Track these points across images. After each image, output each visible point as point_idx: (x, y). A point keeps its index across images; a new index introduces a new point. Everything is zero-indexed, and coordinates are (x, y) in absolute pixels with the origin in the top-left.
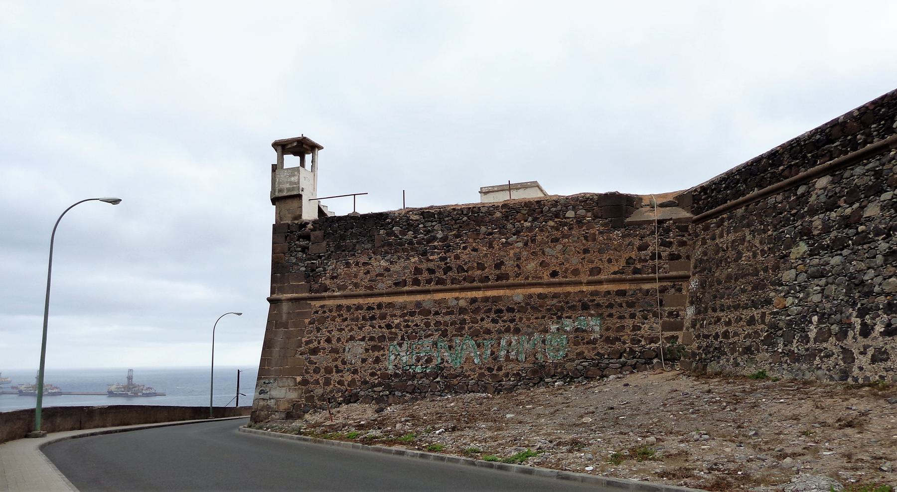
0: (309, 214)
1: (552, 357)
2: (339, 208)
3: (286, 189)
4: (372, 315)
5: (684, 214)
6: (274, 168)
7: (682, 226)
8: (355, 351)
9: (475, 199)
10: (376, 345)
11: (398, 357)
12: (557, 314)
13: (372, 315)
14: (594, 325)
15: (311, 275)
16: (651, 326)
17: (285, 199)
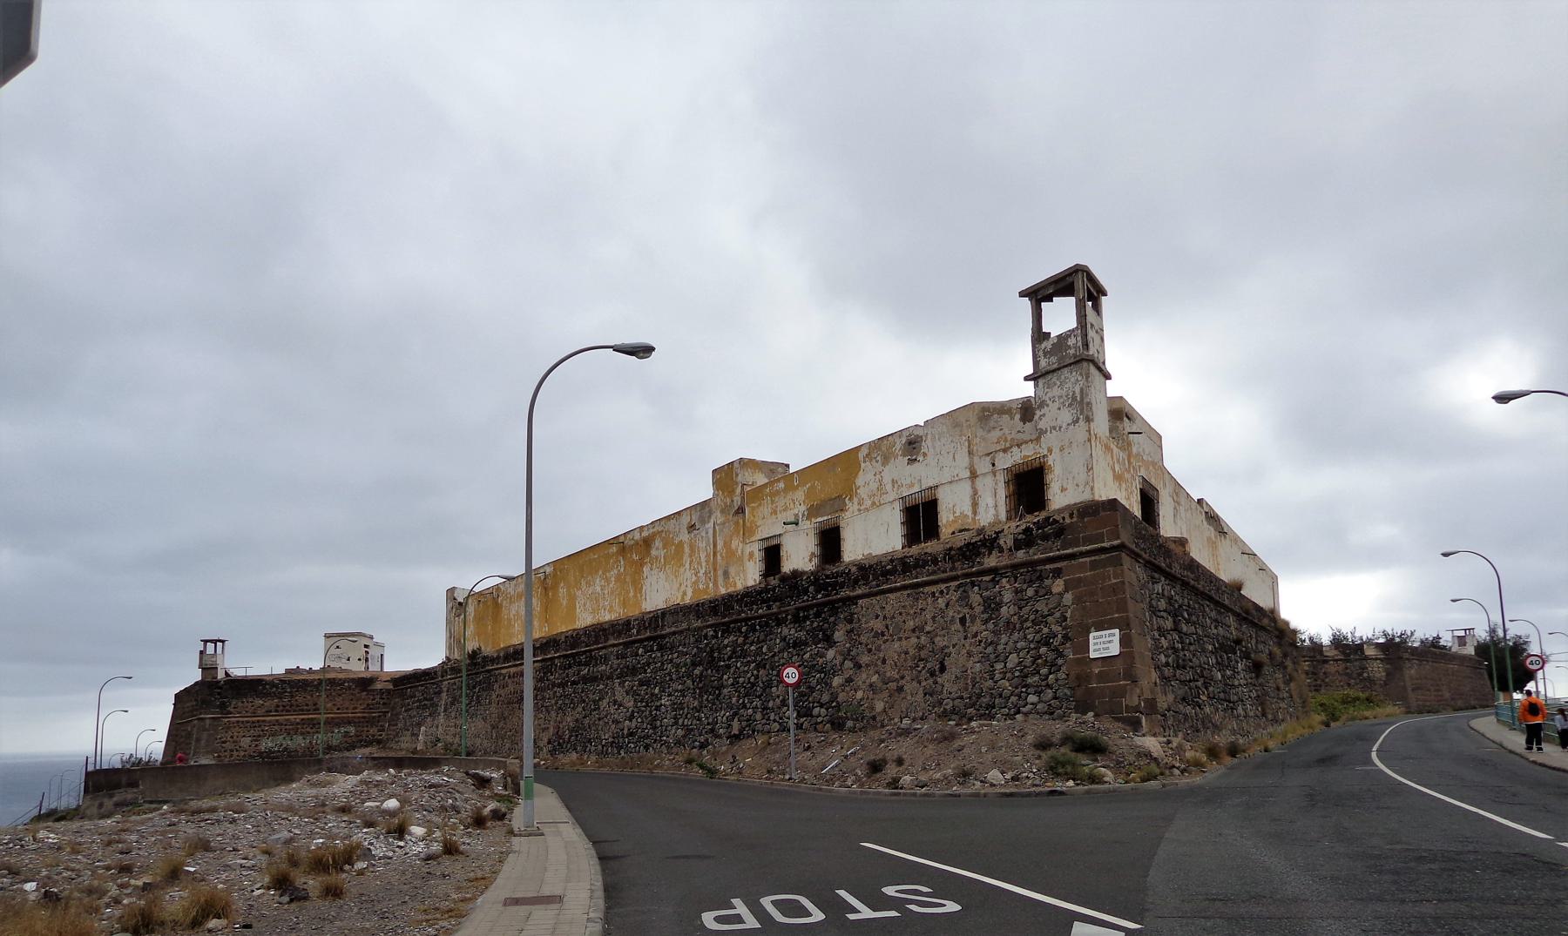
0: (221, 675)
1: (335, 743)
2: (238, 672)
3: (208, 663)
4: (254, 725)
5: (391, 687)
6: (201, 652)
7: (388, 691)
8: (245, 742)
9: (313, 661)
10: (257, 738)
11: (267, 744)
12: (338, 725)
13: (254, 725)
14: (352, 729)
15: (223, 706)
16: (373, 731)
17: (208, 668)
